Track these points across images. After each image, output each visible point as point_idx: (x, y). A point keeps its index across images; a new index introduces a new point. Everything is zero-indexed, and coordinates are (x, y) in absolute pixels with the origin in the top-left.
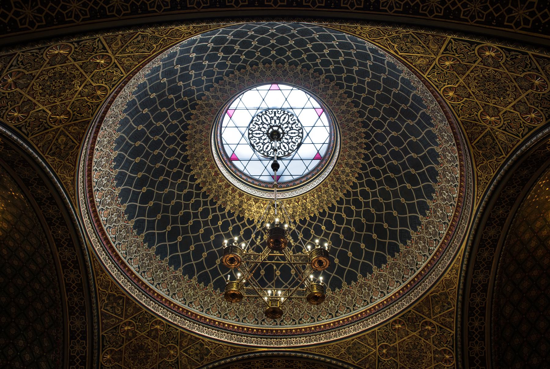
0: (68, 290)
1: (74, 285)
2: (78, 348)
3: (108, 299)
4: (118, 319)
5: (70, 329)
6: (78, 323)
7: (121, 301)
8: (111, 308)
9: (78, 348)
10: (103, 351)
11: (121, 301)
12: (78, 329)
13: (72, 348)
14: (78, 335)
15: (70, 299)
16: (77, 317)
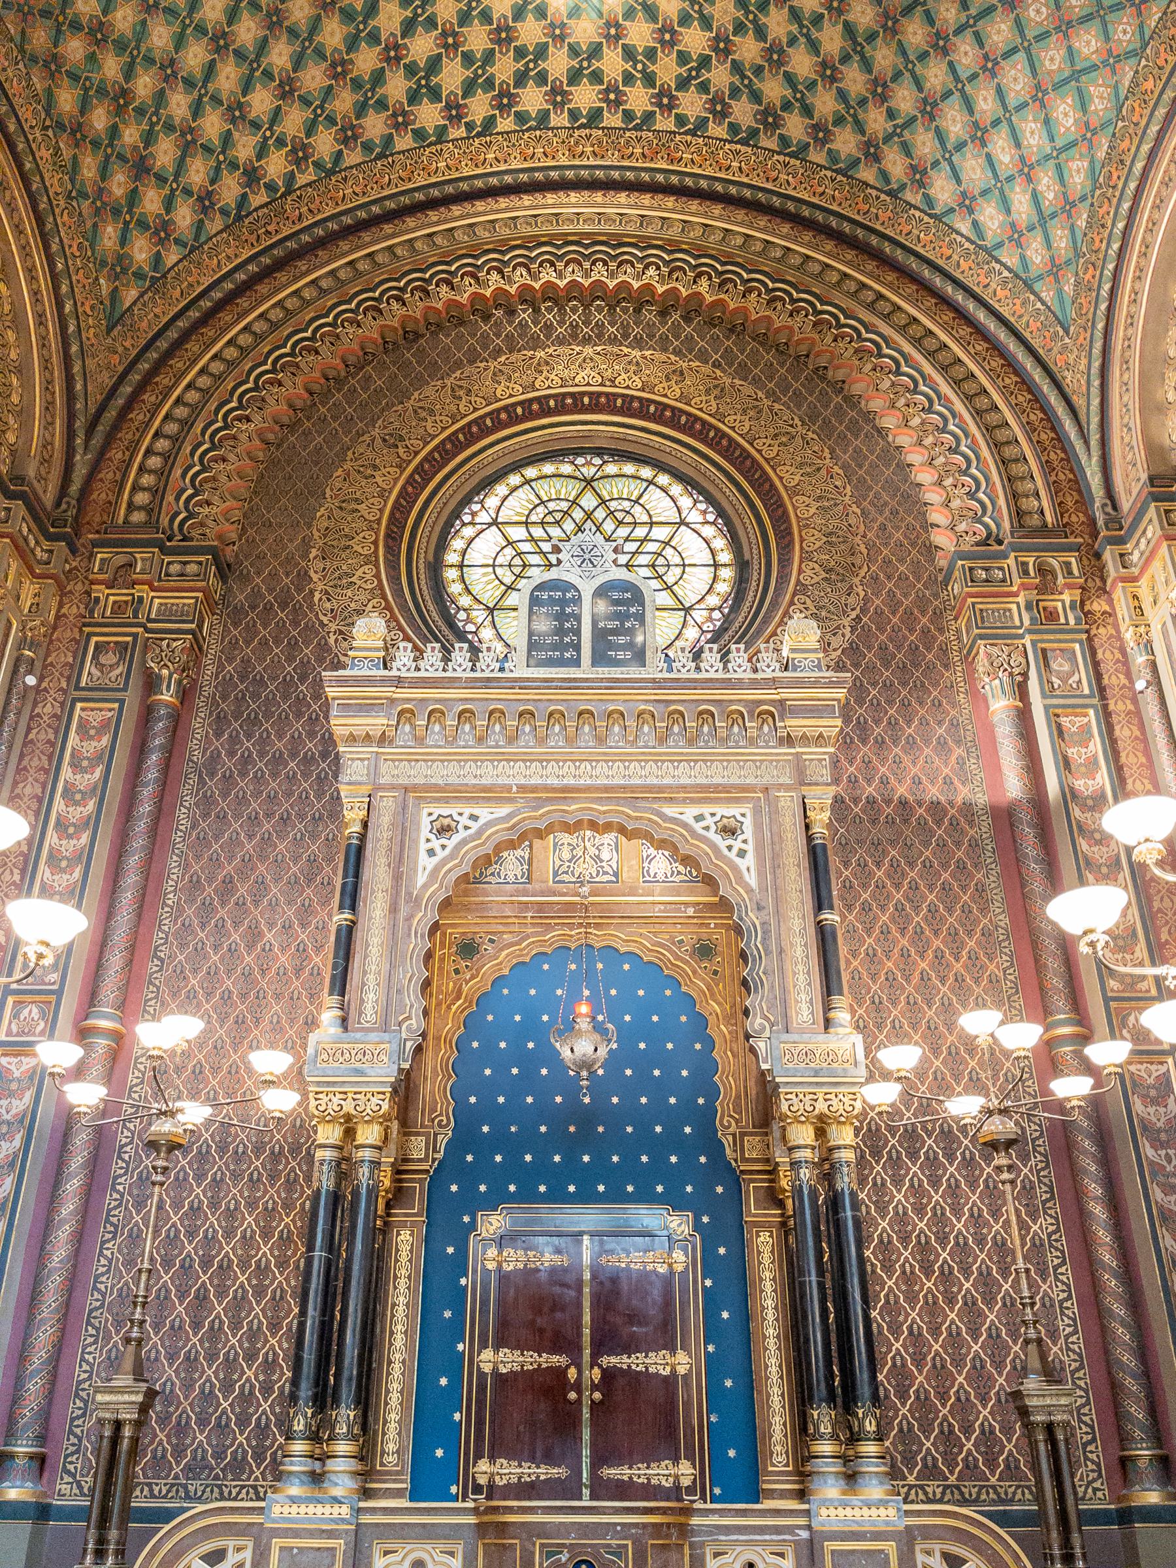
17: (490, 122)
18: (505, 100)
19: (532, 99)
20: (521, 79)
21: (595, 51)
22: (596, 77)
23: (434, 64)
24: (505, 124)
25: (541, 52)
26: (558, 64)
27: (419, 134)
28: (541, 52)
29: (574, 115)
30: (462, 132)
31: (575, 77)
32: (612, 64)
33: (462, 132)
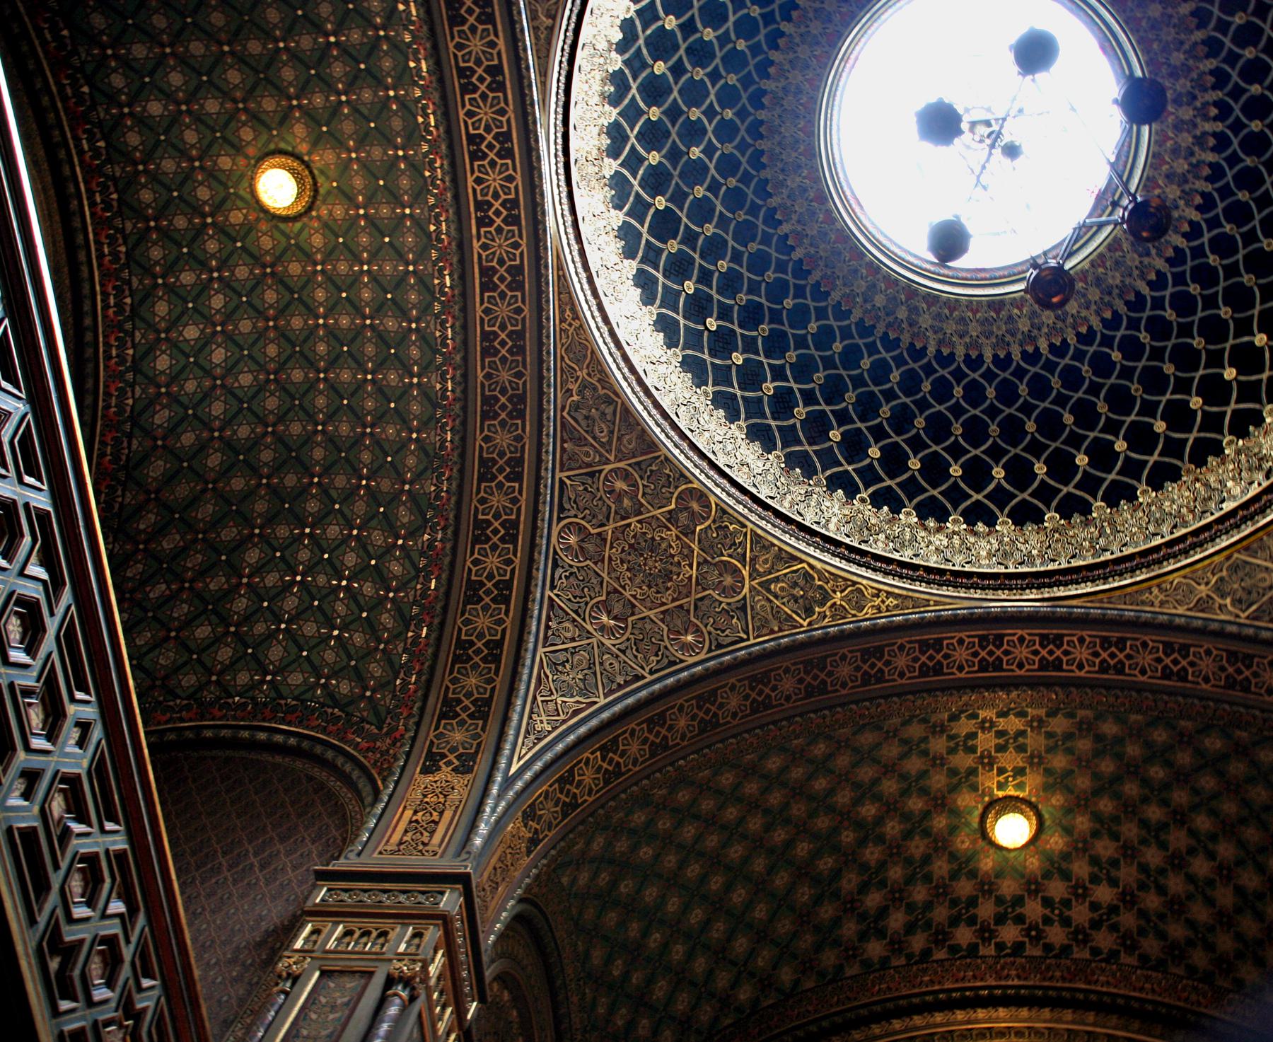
0: (486, 352)
1: (503, 336)
2: (497, 501)
3: (580, 393)
4: (601, 455)
5: (481, 456)
6: (503, 439)
7: (609, 410)
8: (587, 418)
9: (497, 501)
10: (560, 519)
11: (609, 410)
12: (501, 454)
13: (483, 501)
14: (501, 470)
15: (488, 376)
16: (503, 424)
17: (926, 953)
18: (941, 937)
19: (964, 936)
20: (954, 921)
21: (1018, 901)
22: (1020, 919)
23: (883, 912)
24: (940, 954)
25: (972, 902)
26: (986, 910)
27: (867, 964)
28: (972, 902)
29: (1000, 946)
30: (903, 961)
31: (1000, 919)
32: (1034, 910)
33: (903, 961)
